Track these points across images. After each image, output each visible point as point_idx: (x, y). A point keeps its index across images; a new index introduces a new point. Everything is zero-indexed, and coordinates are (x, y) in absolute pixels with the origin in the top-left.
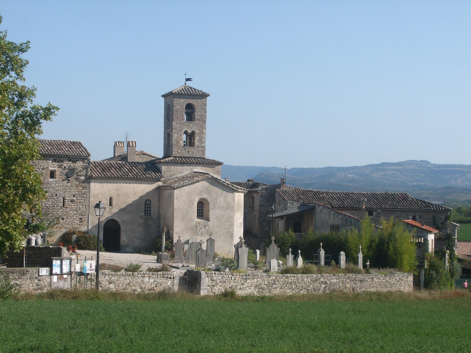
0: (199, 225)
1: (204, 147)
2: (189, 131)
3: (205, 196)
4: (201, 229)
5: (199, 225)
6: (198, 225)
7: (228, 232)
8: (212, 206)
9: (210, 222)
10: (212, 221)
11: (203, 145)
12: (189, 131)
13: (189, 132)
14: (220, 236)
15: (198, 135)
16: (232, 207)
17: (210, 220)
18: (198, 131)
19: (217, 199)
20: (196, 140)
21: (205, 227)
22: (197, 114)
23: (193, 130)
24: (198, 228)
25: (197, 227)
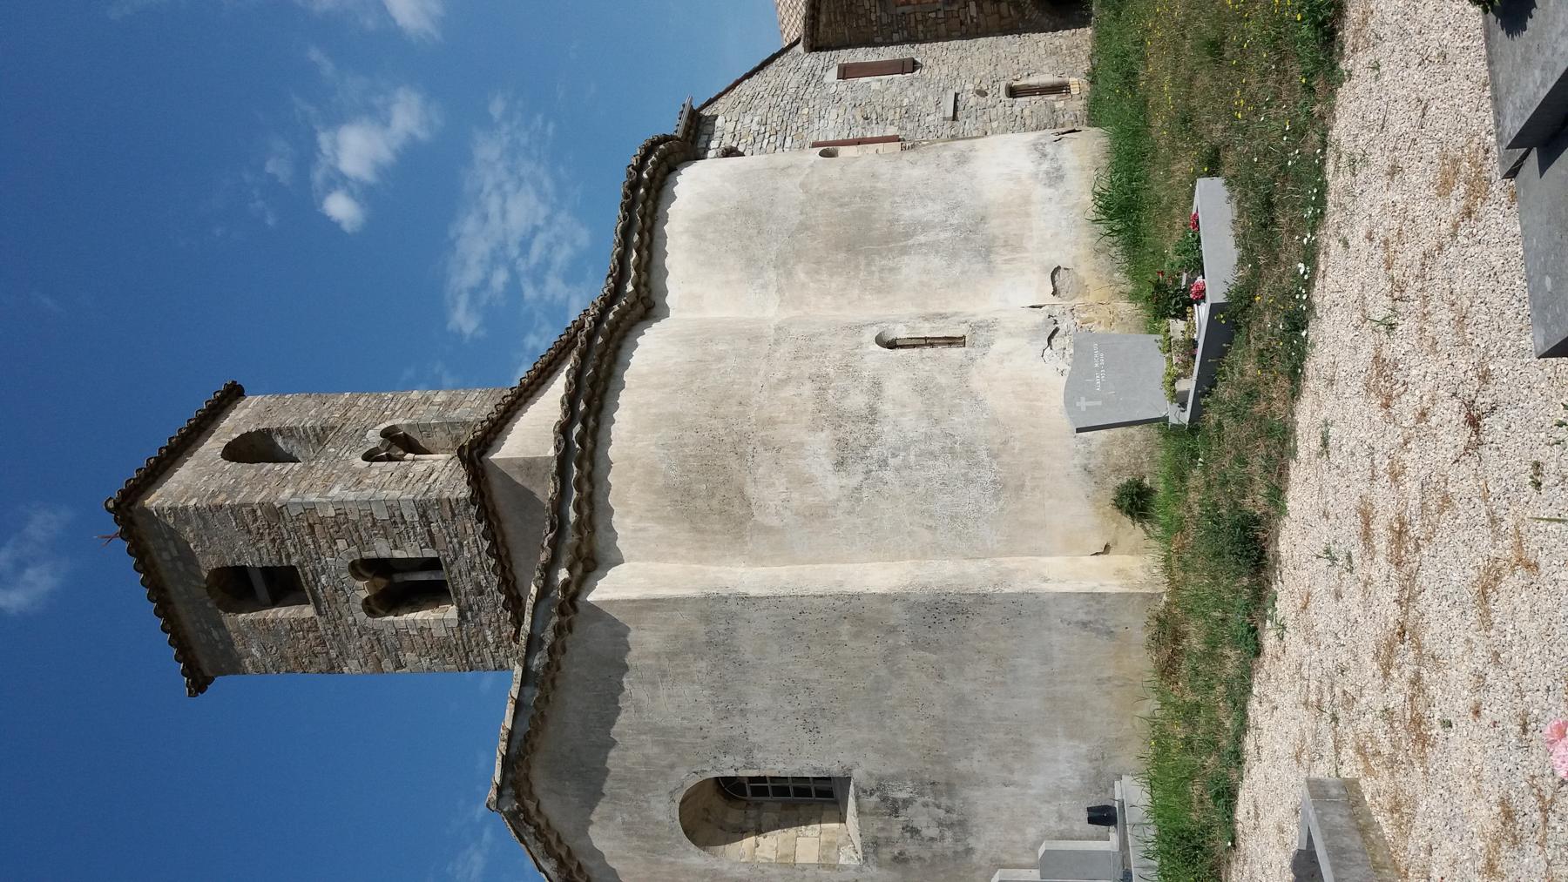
0: (889, 842)
1: (423, 509)
2: (362, 590)
3: (665, 811)
4: (914, 831)
5: (889, 842)
6: (886, 854)
7: (916, 644)
8: (729, 760)
9: (857, 775)
10: (847, 759)
11: (411, 515)
12: (362, 590)
13: (364, 594)
14: (961, 701)
15: (363, 544)
16: (706, 619)
17: (835, 770)
18: (341, 544)
19: (664, 731)
20: (397, 554)
21: (894, 808)
22: (254, 555)
23: (345, 575)
24: (912, 849)
25: (901, 859)
